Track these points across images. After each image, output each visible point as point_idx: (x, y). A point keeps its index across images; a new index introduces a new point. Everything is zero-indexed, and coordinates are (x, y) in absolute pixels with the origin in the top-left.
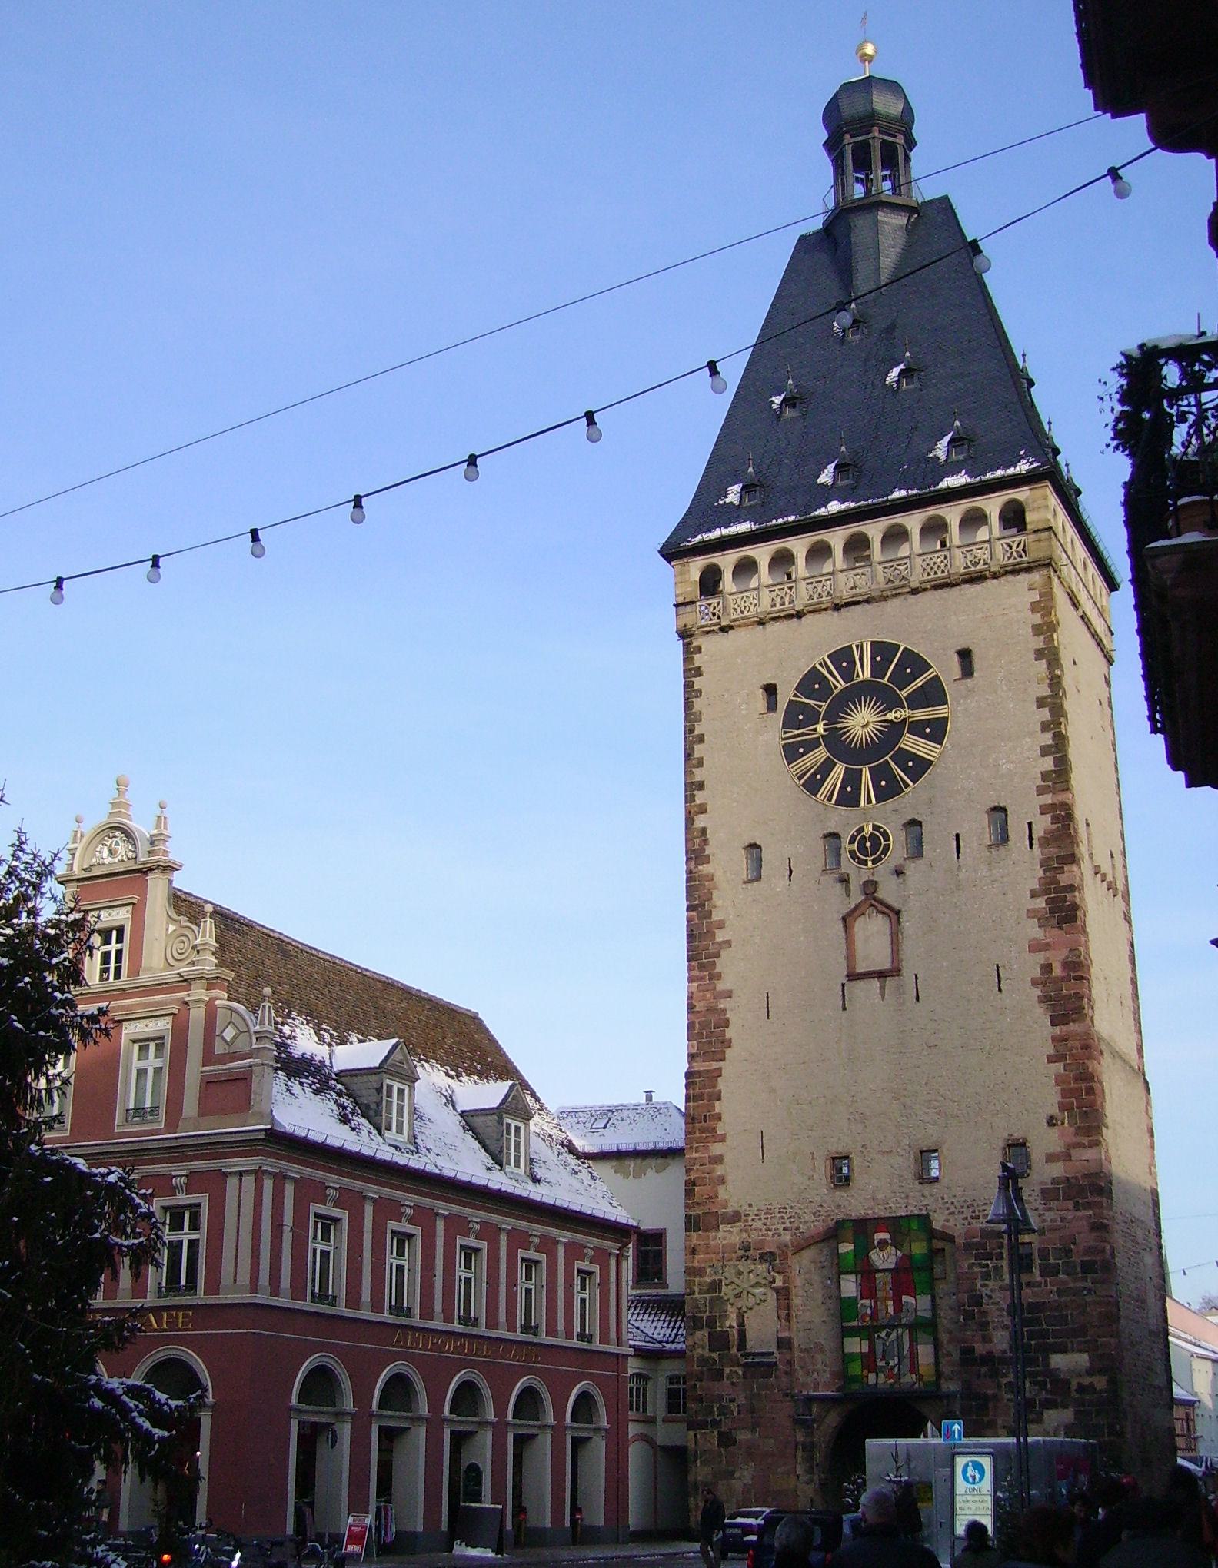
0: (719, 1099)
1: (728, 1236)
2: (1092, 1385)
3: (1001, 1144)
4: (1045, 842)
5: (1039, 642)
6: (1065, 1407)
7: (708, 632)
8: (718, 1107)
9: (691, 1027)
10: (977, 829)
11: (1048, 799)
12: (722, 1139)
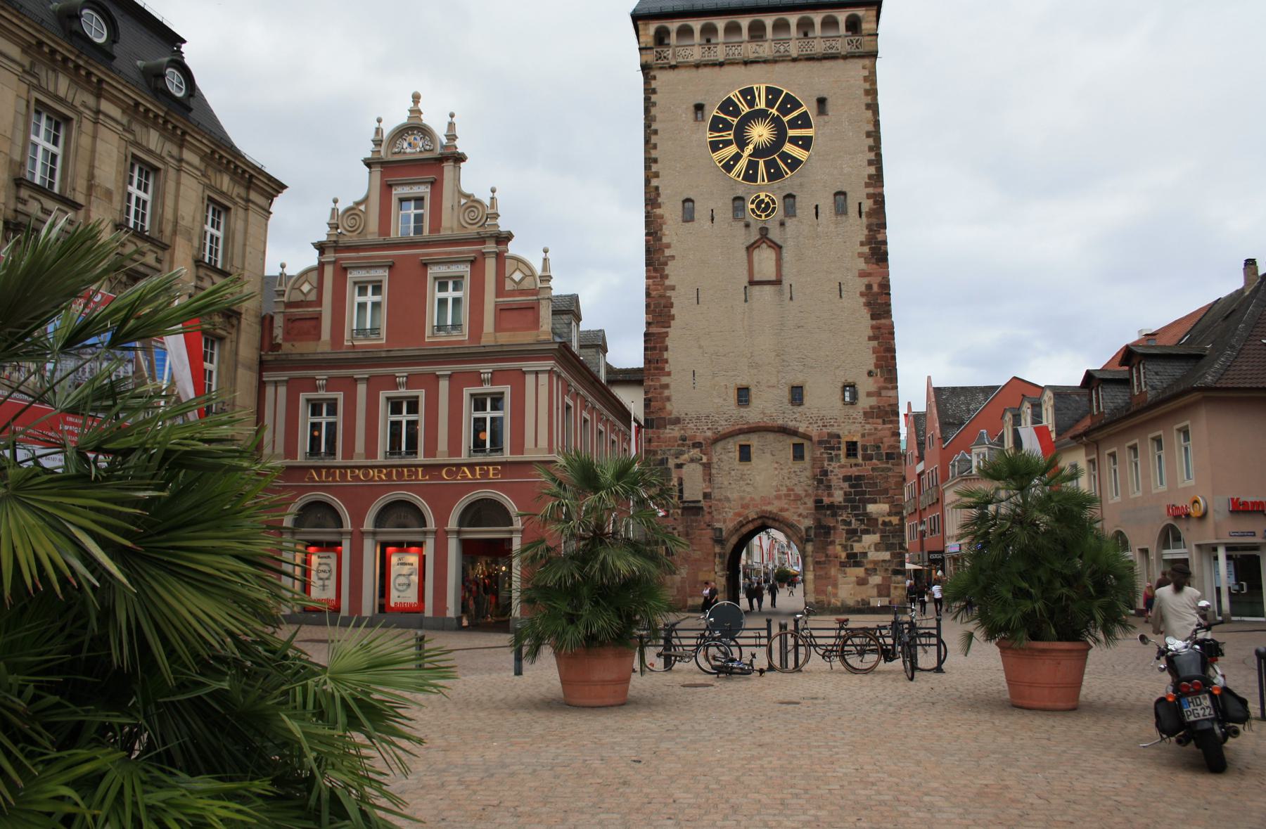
0: (666, 349)
1: (672, 432)
3: (841, 385)
4: (869, 215)
5: (868, 100)
8: (666, 355)
9: (648, 306)
10: (827, 205)
11: (871, 190)
12: (669, 374)
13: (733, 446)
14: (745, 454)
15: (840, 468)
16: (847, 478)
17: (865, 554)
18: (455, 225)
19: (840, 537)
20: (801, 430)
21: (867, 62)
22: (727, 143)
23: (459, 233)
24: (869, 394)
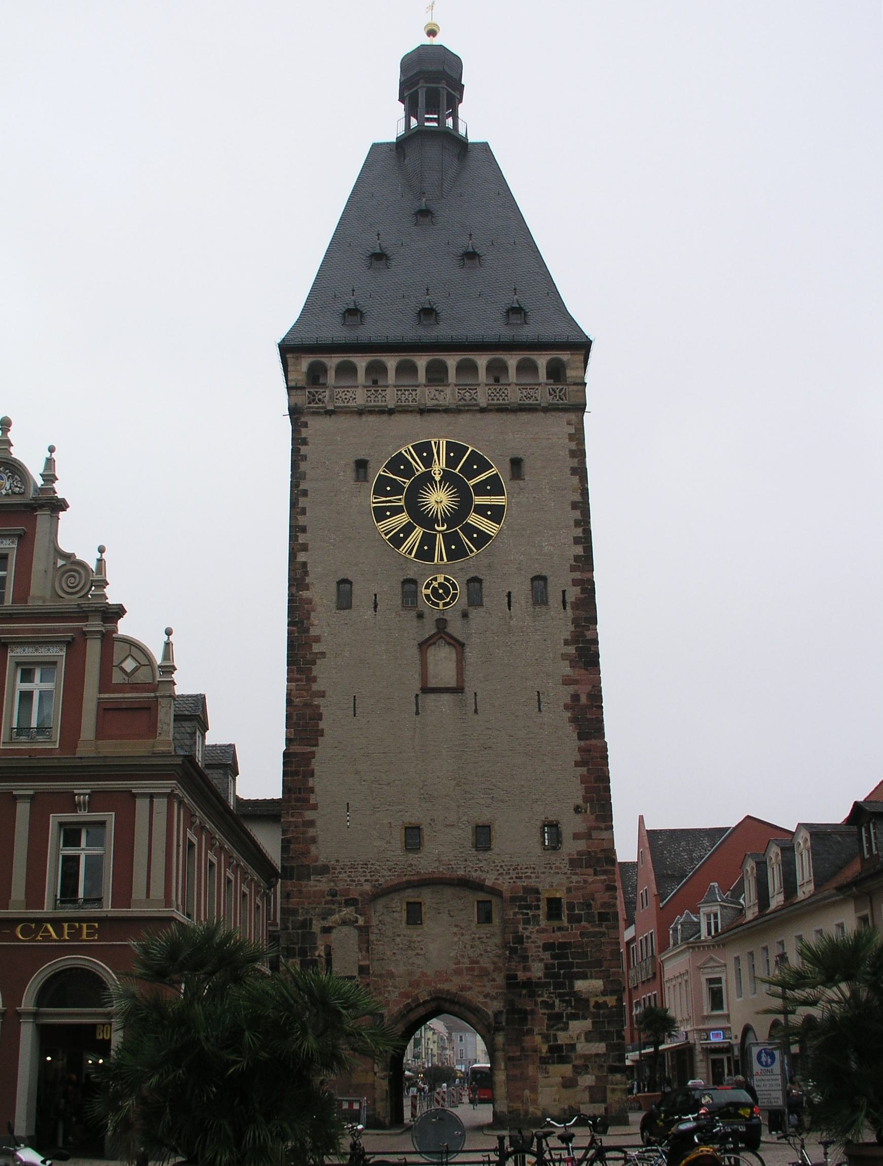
0: (312, 774)
1: (318, 884)
2: (605, 1002)
3: (539, 824)
4: (576, 606)
6: (585, 1018)
7: (315, 413)
9: (289, 717)
10: (522, 590)
11: (577, 575)
12: (315, 807)
13: (398, 904)
14: (414, 915)
15: (538, 934)
16: (547, 947)
17: (573, 1047)
18: (48, 594)
19: (539, 1025)
20: (488, 883)
21: (572, 416)
22: (396, 511)
23: (52, 605)
24: (576, 836)
